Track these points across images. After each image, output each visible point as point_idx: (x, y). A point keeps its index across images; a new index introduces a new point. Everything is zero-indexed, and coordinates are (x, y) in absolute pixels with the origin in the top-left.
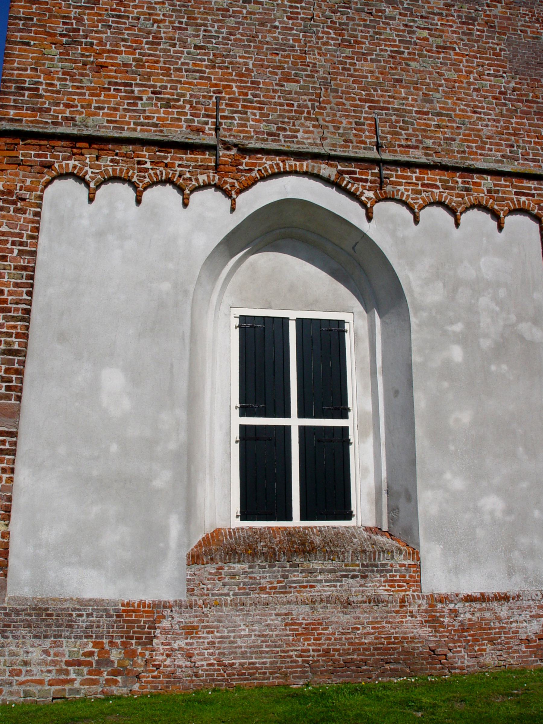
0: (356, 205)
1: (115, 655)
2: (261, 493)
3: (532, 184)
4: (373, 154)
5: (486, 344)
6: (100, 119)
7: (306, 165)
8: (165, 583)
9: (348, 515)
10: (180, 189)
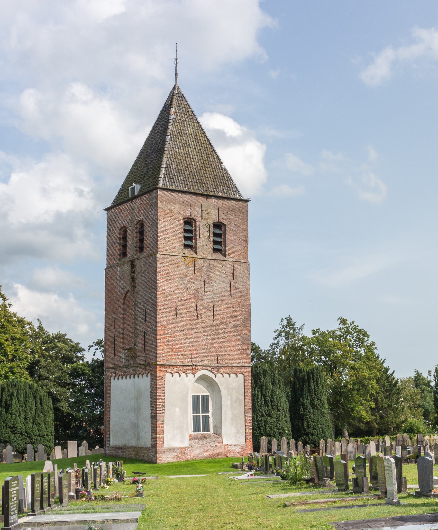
0: (213, 374)
1: (180, 456)
3: (243, 368)
4: (217, 365)
5: (234, 400)
6: (173, 361)
7: (206, 368)
8: (186, 444)
9: (209, 431)
10: (186, 374)
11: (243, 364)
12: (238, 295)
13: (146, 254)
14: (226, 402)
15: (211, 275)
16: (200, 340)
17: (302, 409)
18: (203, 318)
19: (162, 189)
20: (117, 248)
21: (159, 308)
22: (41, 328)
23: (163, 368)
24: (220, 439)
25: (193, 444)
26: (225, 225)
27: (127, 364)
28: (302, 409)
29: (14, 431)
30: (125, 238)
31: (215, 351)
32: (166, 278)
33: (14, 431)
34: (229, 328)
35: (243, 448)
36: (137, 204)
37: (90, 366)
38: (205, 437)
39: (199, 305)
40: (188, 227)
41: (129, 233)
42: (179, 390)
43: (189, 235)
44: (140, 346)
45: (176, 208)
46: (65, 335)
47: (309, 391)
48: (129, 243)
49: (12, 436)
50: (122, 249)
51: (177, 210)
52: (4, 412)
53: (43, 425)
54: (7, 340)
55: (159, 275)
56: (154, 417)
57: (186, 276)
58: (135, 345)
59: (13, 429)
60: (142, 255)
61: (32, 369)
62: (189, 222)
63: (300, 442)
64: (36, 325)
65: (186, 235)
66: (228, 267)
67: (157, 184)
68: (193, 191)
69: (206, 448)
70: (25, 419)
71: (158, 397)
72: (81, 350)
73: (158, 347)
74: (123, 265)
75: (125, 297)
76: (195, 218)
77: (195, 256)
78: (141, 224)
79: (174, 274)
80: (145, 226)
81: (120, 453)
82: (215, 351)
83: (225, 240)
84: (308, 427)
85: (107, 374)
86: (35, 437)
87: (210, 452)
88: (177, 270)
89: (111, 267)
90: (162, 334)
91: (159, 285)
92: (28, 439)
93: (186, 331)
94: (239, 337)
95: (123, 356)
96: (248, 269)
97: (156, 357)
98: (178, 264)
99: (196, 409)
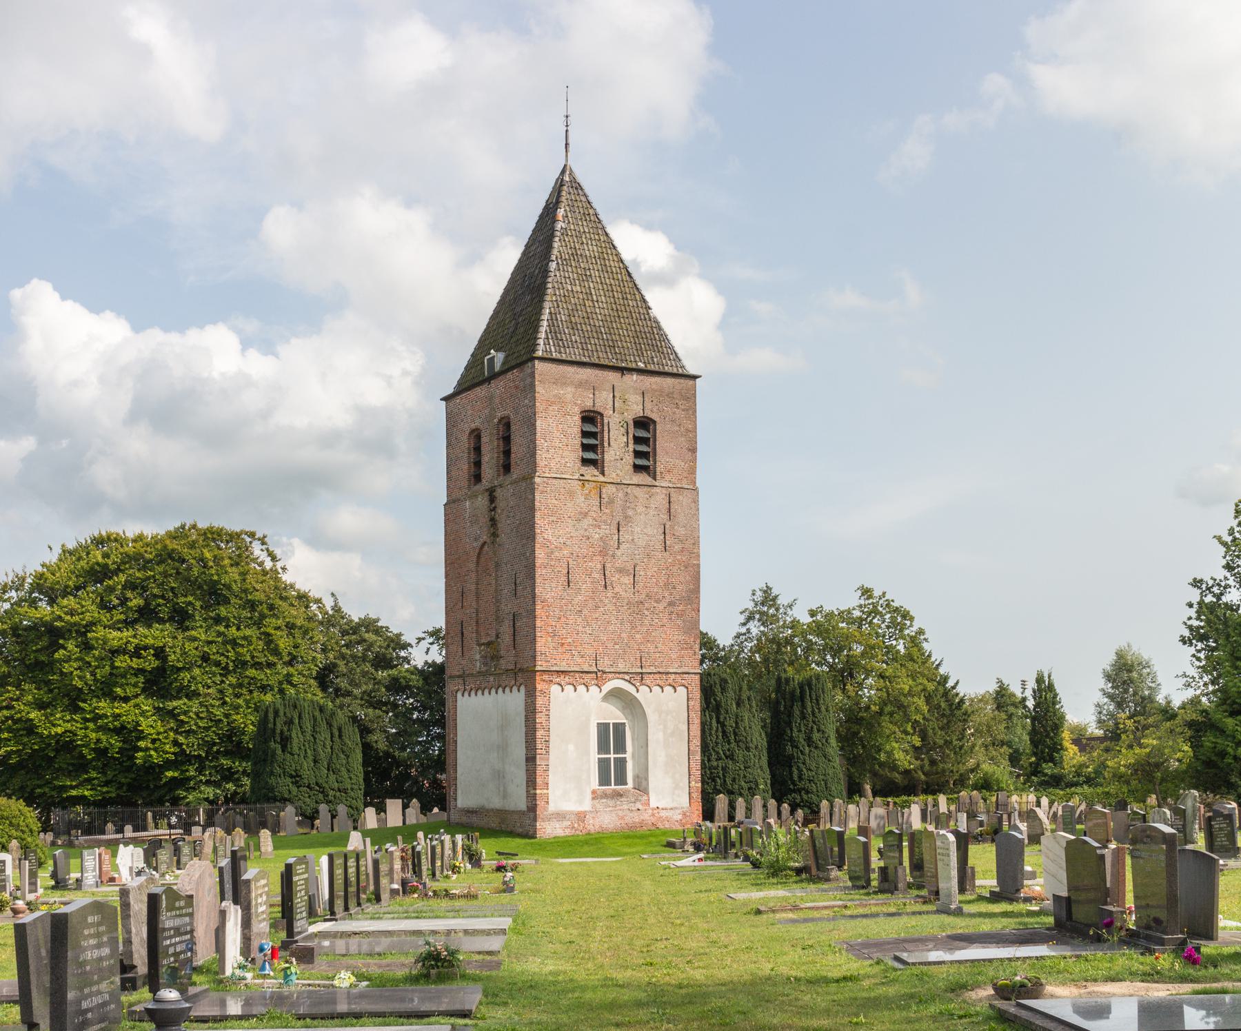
2: (604, 780)
4: (640, 670)
8: (586, 805)
11: (686, 670)
12: (677, 547)
13: (515, 476)
14: (656, 735)
15: (630, 513)
16: (611, 628)
17: (789, 748)
18: (616, 590)
19: (541, 359)
20: (464, 467)
21: (538, 572)
22: (337, 609)
23: (546, 677)
24: (645, 797)
25: (598, 806)
26: (654, 422)
27: (484, 669)
28: (789, 748)
29: (297, 782)
30: (478, 449)
31: (636, 647)
32: (551, 519)
33: (297, 782)
34: (661, 606)
35: (684, 814)
36: (498, 387)
37: (421, 672)
38: (619, 795)
39: (608, 565)
40: (589, 428)
41: (484, 439)
42: (573, 715)
43: (592, 441)
44: (506, 639)
45: (568, 392)
46: (378, 620)
47: (803, 717)
48: (486, 458)
49: (294, 789)
50: (473, 470)
51: (569, 396)
52: (279, 752)
53: (344, 772)
54: (278, 628)
55: (538, 515)
56: (531, 759)
57: (586, 515)
58: (497, 637)
59: (296, 778)
60: (509, 479)
61: (324, 678)
62: (590, 418)
63: (786, 805)
64: (328, 604)
65: (585, 441)
66: (660, 498)
67: (534, 351)
68: (597, 361)
69: (620, 813)
70: (315, 761)
71: (538, 726)
72: (405, 646)
73: (538, 639)
74: (476, 496)
75: (479, 554)
76: (601, 410)
77: (601, 478)
78: (506, 424)
79: (565, 511)
80: (513, 428)
81: (474, 820)
82: (636, 647)
83: (655, 449)
84: (800, 778)
85: (450, 686)
86: (331, 793)
87: (628, 820)
88: (569, 505)
89: (454, 501)
90: (544, 618)
91: (538, 531)
92: (321, 796)
93: (585, 612)
94: (679, 622)
95: (478, 657)
96: (696, 501)
97: (534, 657)
98: (571, 494)
99: (603, 746)
